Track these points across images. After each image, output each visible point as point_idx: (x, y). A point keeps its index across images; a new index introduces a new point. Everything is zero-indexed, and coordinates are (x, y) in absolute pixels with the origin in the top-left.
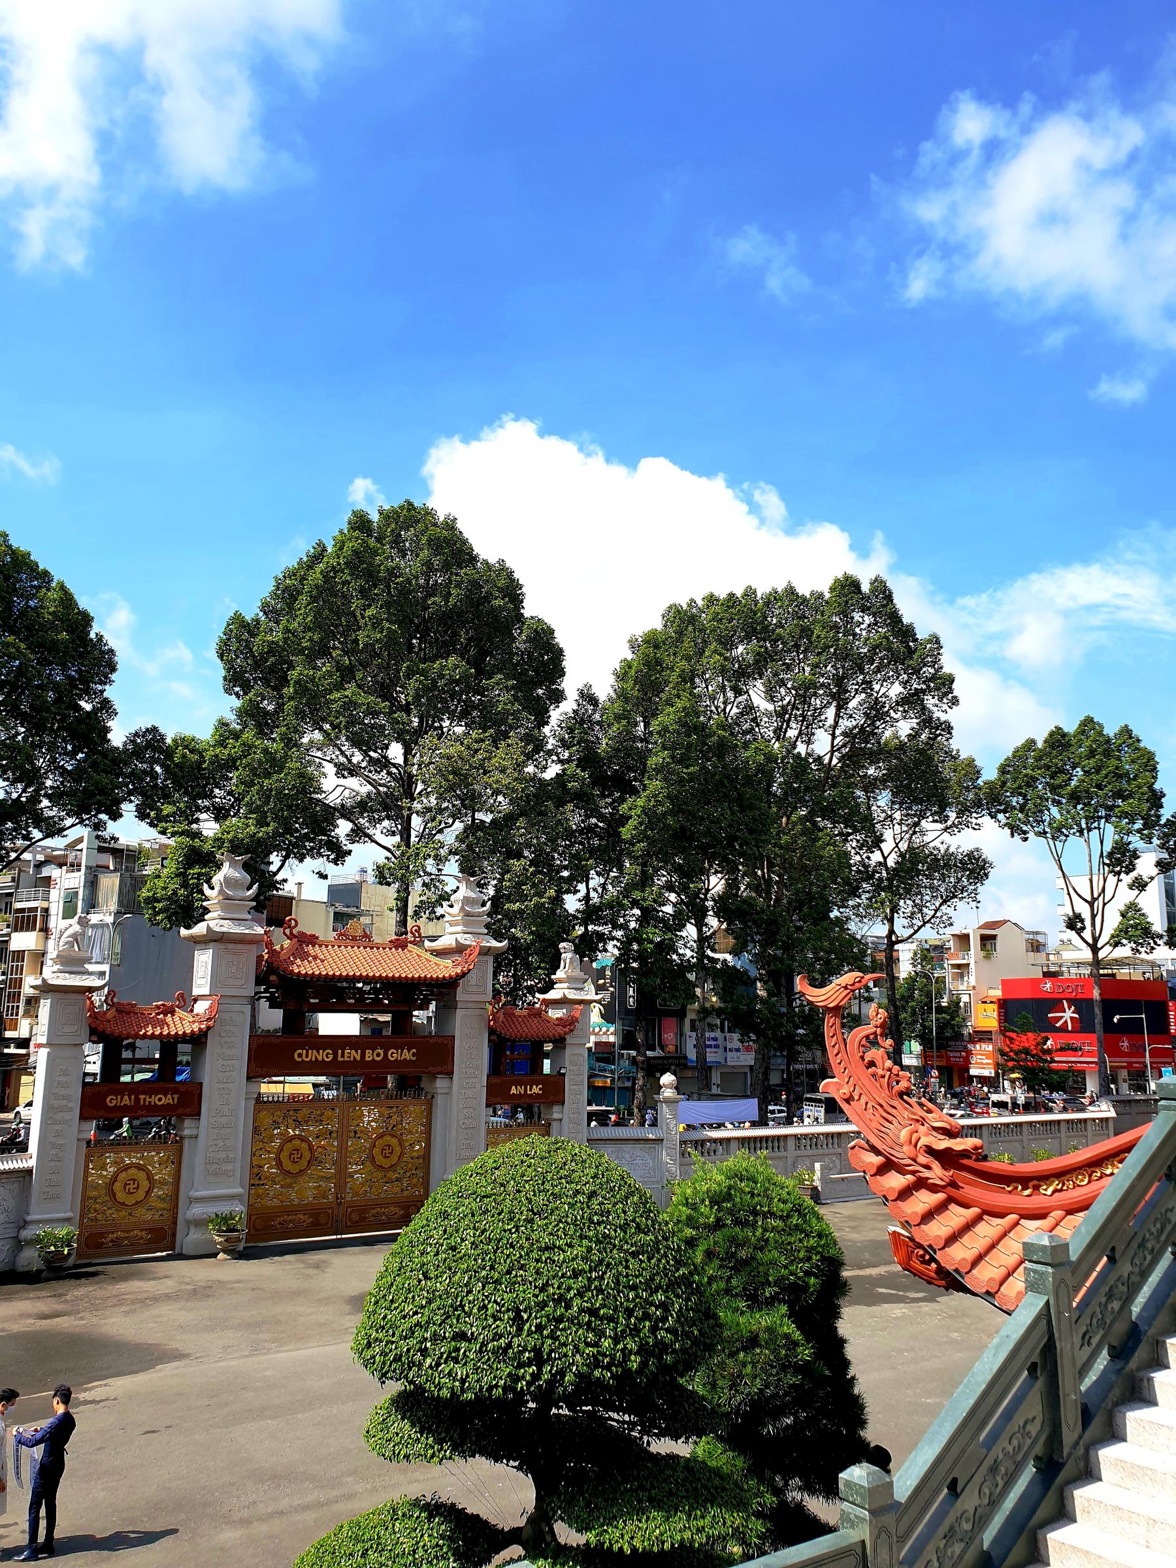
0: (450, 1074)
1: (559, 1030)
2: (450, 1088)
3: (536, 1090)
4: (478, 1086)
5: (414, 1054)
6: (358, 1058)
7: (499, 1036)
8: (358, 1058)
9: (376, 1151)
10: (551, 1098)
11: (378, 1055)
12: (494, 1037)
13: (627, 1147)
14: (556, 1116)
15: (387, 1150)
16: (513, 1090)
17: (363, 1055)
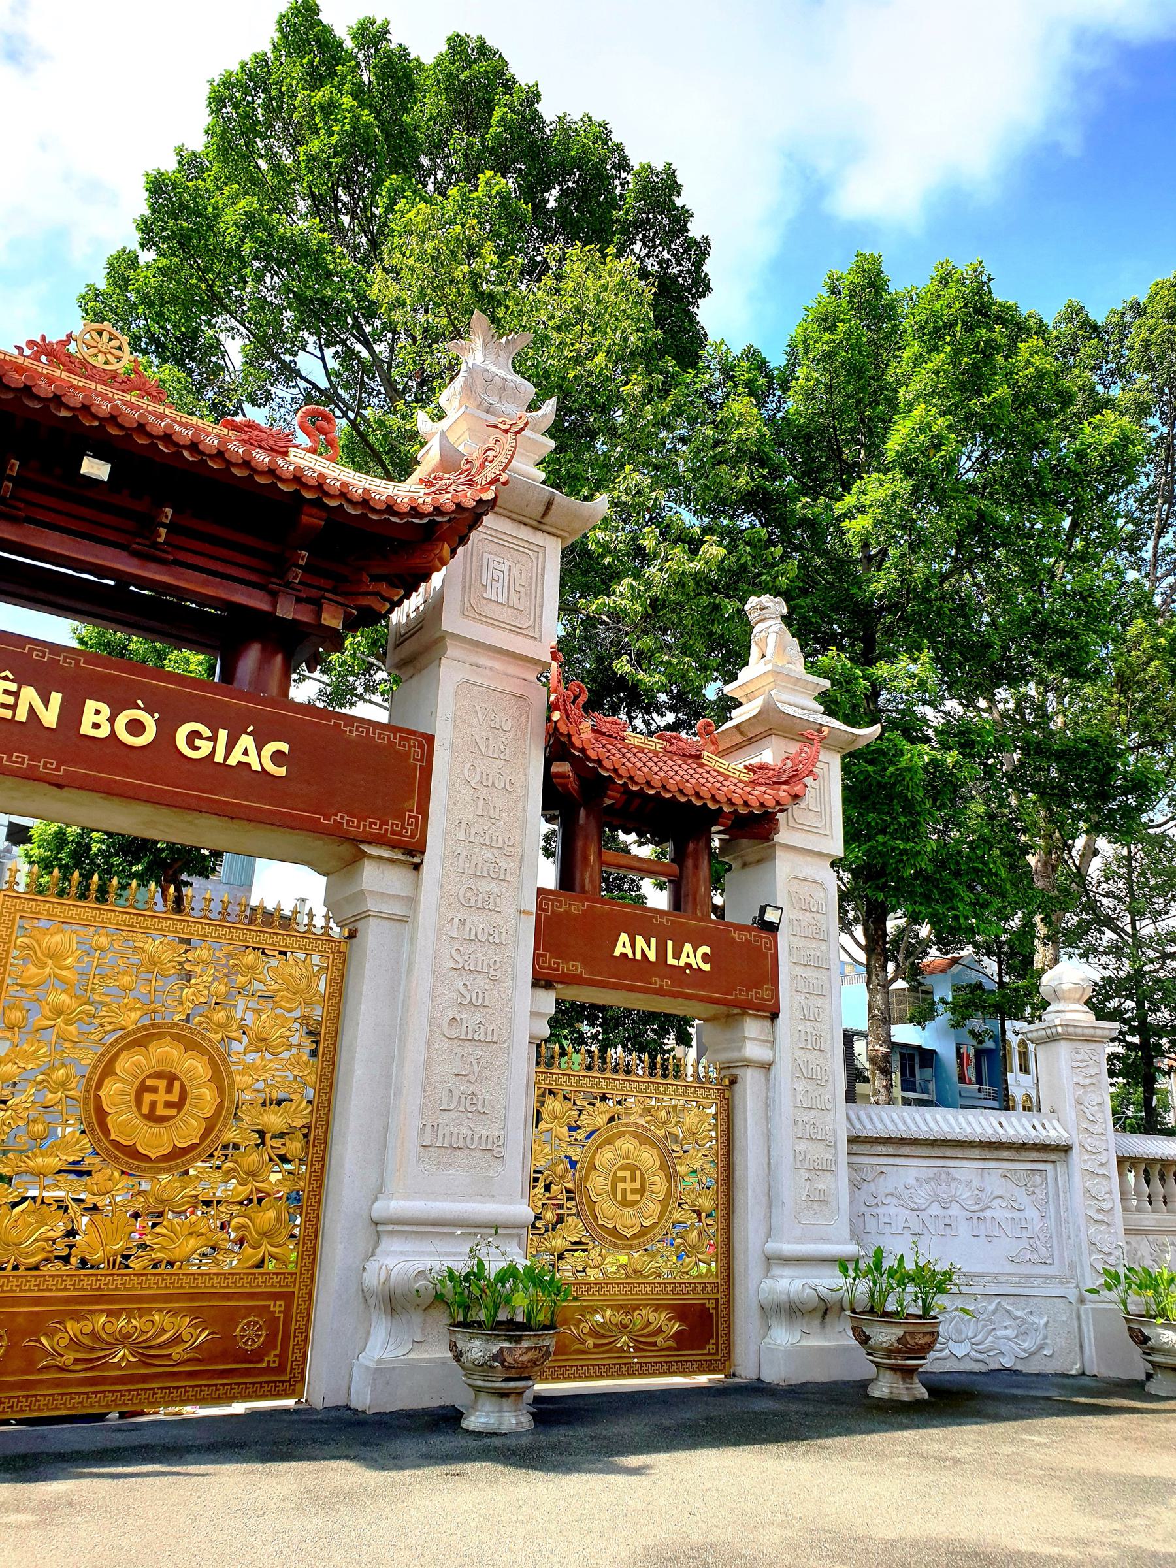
0: (412, 852)
1: (760, 795)
2: (412, 901)
3: (693, 957)
4: (509, 911)
5: (277, 757)
6: (50, 717)
7: (579, 763)
8: (50, 717)
9: (111, 1090)
10: (739, 993)
11: (136, 727)
12: (556, 768)
13: (965, 1170)
14: (754, 1051)
15: (162, 1095)
16: (623, 945)
17: (71, 714)
